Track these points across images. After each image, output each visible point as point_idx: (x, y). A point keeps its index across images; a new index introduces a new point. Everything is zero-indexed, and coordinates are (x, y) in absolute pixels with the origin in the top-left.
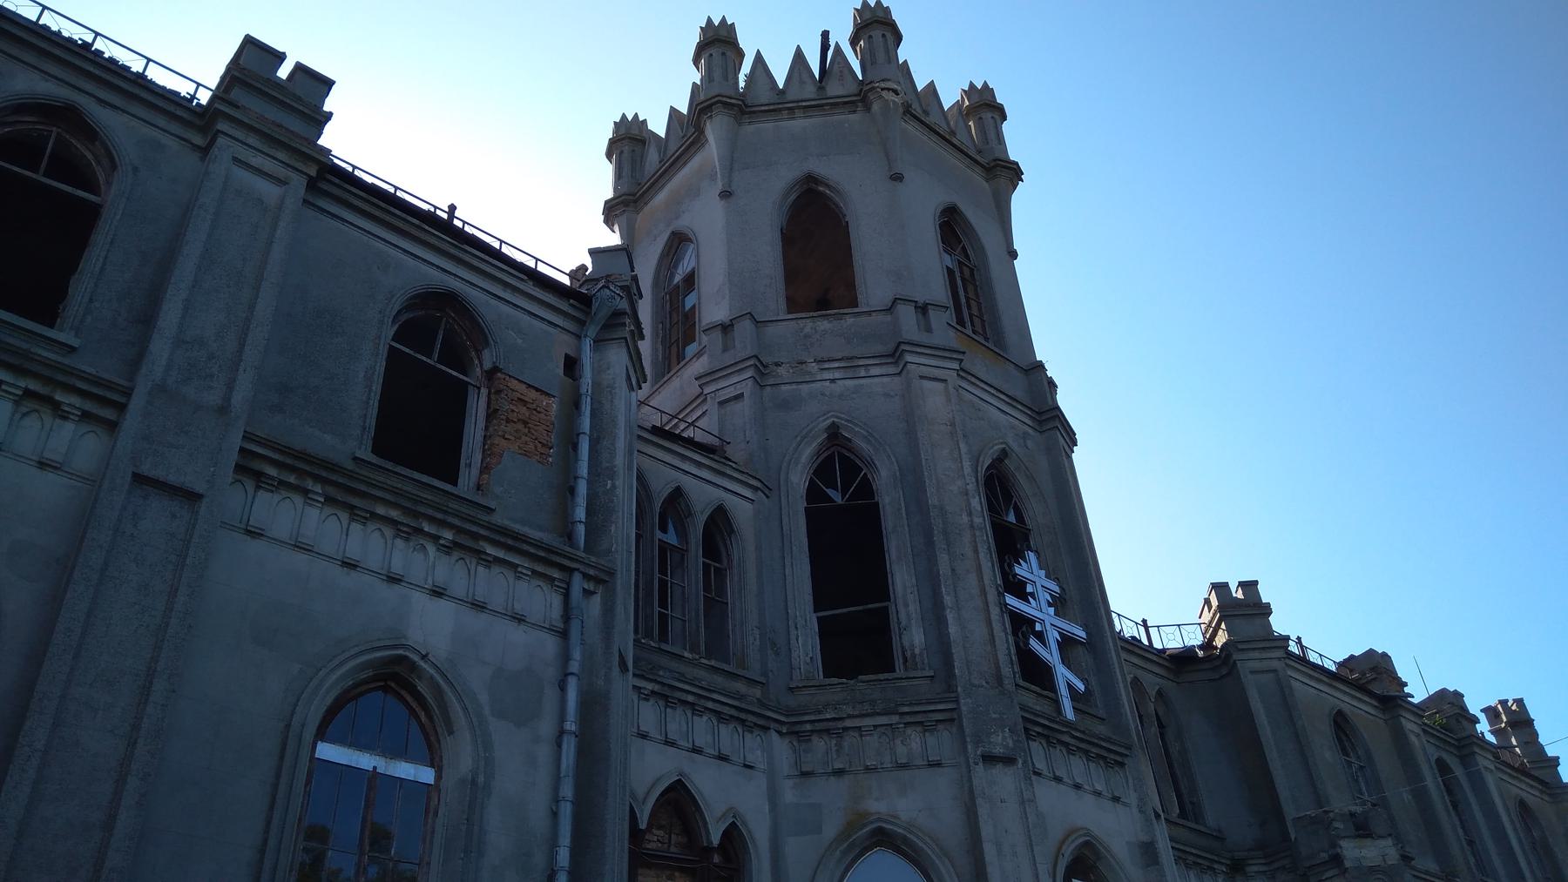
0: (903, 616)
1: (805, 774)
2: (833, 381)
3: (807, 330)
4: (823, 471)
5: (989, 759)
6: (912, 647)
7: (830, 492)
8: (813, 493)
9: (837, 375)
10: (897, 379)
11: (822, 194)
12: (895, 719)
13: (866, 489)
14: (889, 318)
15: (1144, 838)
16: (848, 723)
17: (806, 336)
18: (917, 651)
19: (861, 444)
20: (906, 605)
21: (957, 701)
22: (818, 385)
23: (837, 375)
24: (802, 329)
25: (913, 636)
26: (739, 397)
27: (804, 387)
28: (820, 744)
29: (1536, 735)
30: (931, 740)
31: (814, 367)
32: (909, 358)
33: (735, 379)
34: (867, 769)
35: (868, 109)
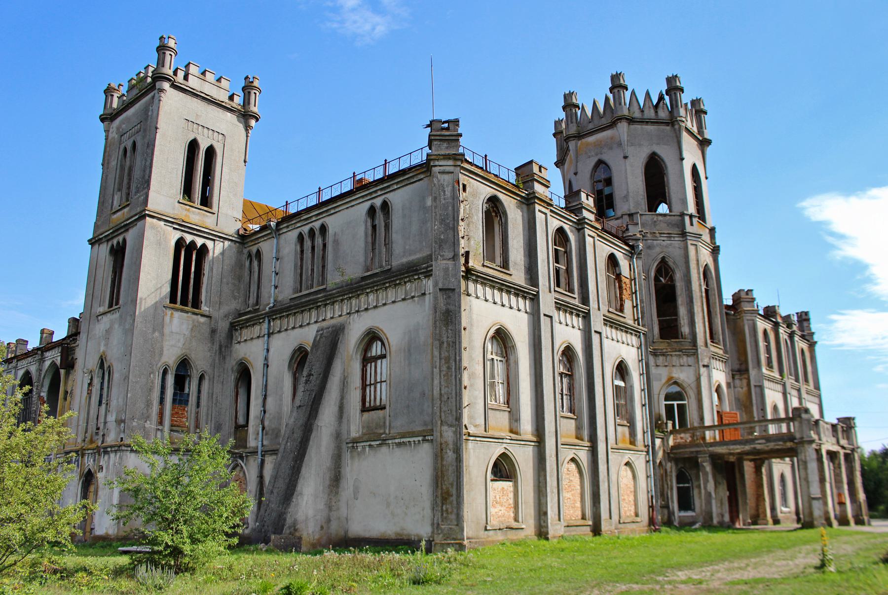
0: (682, 322)
1: (657, 366)
2: (664, 241)
3: (655, 219)
4: (659, 271)
5: (704, 366)
6: (685, 332)
7: (661, 278)
8: (656, 279)
9: (665, 239)
10: (683, 242)
11: (655, 159)
12: (680, 353)
13: (672, 279)
14: (680, 218)
15: (729, 381)
16: (669, 353)
17: (655, 222)
18: (686, 334)
19: (671, 264)
20: (683, 319)
21: (697, 350)
23: (665, 239)
24: (653, 219)
25: (685, 329)
27: (655, 242)
28: (661, 358)
29: (809, 324)
30: (689, 359)
31: (658, 235)
32: (688, 238)
34: (673, 366)
35: (673, 125)
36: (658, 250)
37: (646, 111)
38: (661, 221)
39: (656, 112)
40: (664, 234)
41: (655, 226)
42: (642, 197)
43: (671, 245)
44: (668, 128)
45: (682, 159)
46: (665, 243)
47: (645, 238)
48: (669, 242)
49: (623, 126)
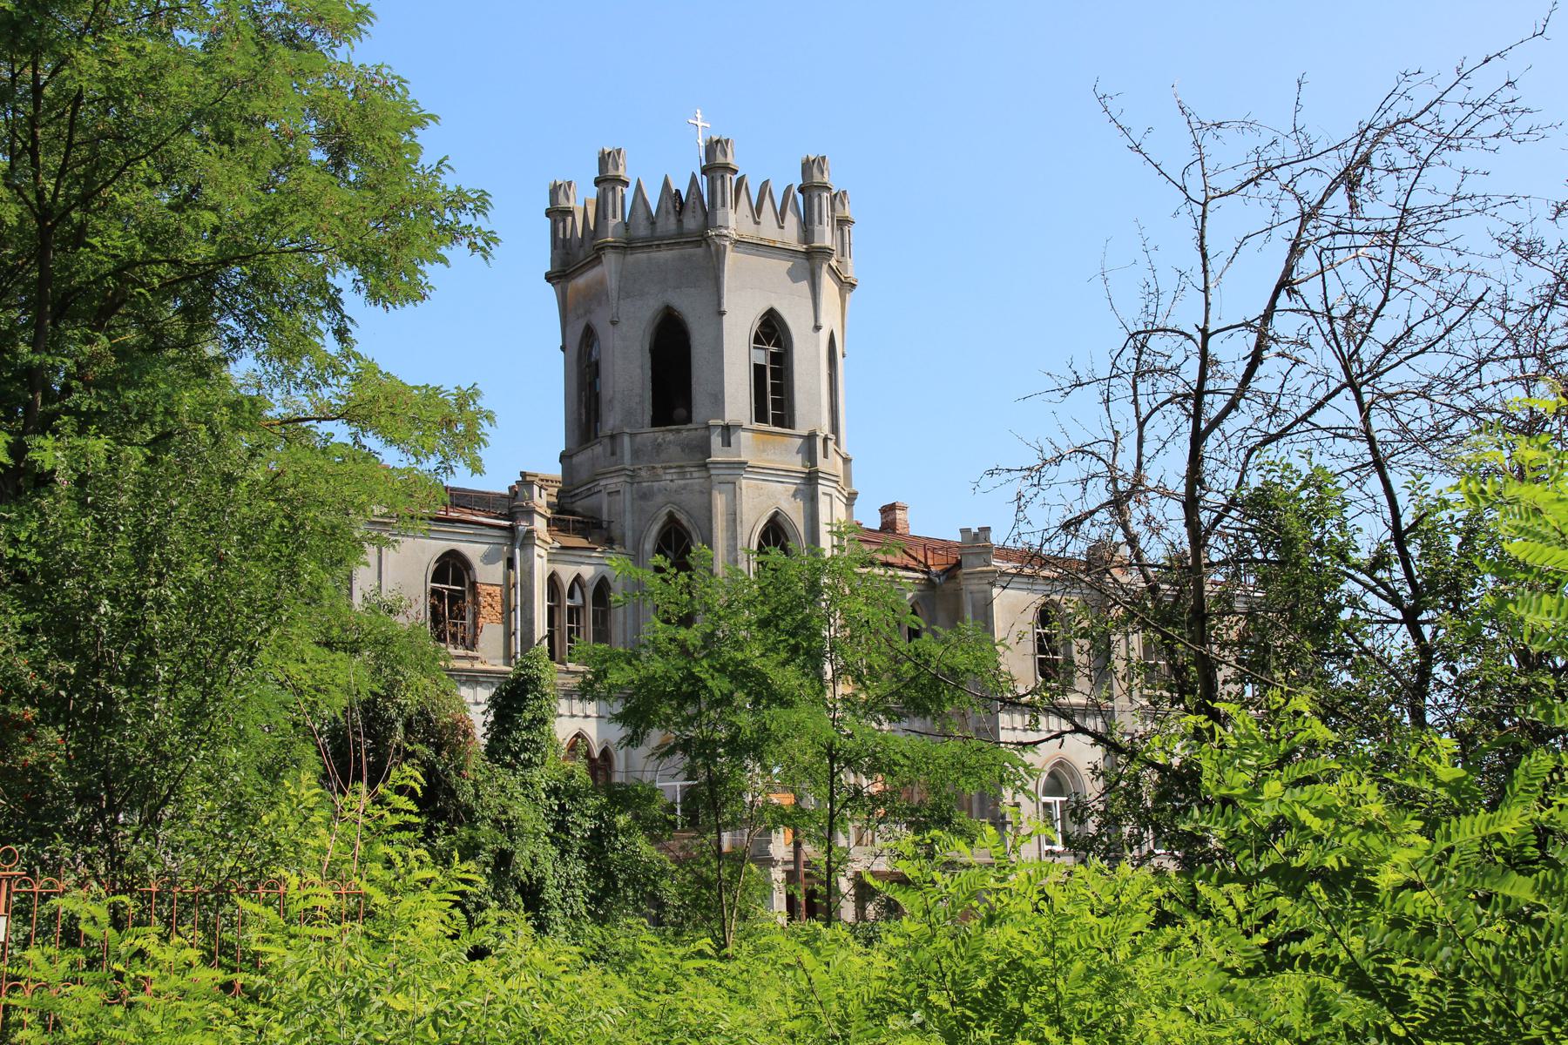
3: (660, 440)
24: (656, 439)
26: (618, 492)
31: (660, 472)
33: (615, 480)
36: (660, 499)
37: (660, 223)
38: (670, 442)
39: (680, 221)
40: (671, 468)
41: (658, 454)
42: (637, 399)
43: (684, 487)
44: (700, 251)
45: (722, 313)
46: (674, 485)
49: (610, 260)
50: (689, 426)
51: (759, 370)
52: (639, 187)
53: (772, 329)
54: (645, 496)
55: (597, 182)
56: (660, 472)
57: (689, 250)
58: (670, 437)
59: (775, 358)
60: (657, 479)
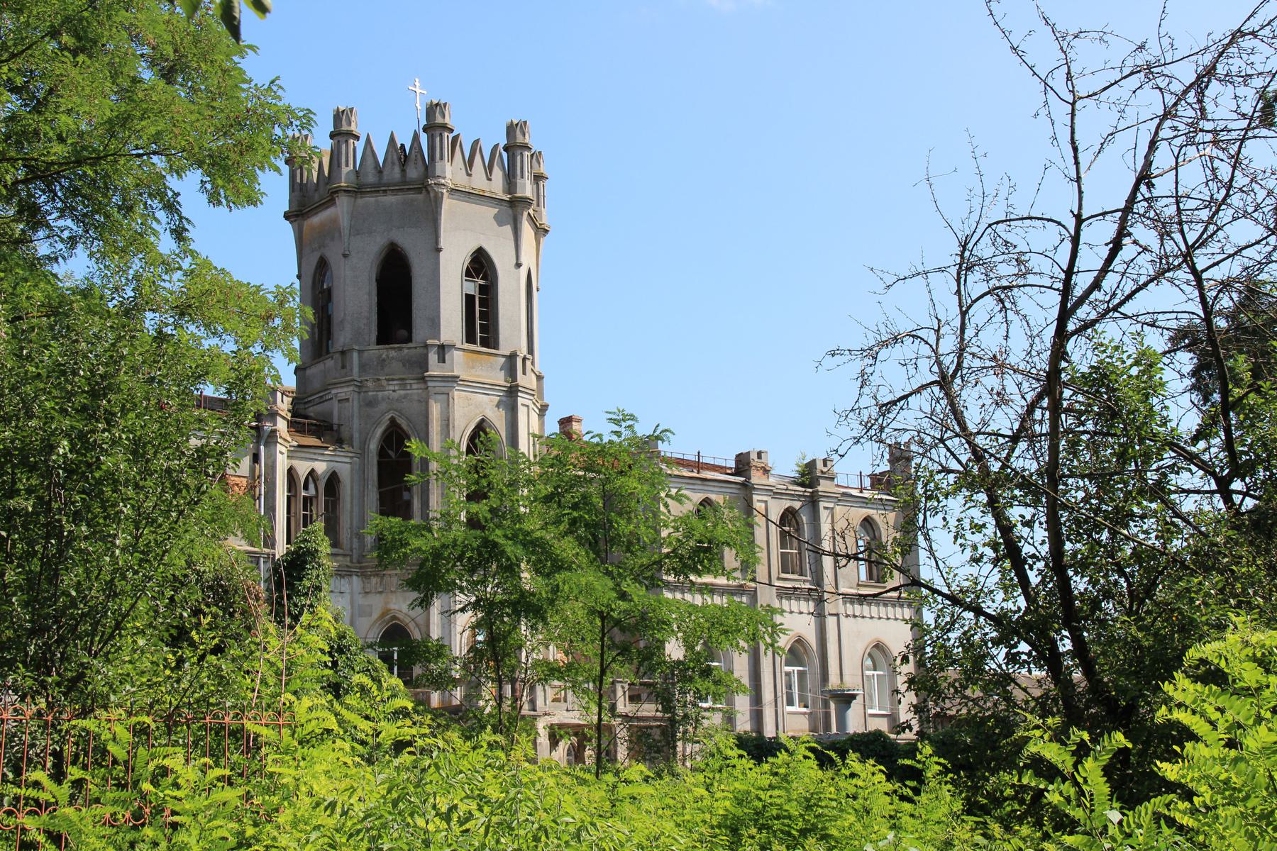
1: (366, 593)
2: (394, 391)
17: (384, 360)
22: (386, 393)
23: (396, 388)
26: (347, 400)
27: (380, 394)
31: (384, 383)
33: (345, 389)
36: (383, 406)
38: (393, 358)
39: (403, 171)
40: (393, 380)
42: (365, 321)
43: (405, 396)
44: (421, 197)
46: (395, 395)
47: (364, 389)
48: (402, 392)
49: (343, 202)
50: (410, 345)
51: (469, 299)
52: (368, 141)
53: (480, 265)
54: (371, 403)
55: (332, 136)
56: (384, 383)
57: (411, 196)
58: (393, 354)
59: (483, 289)
60: (382, 389)
